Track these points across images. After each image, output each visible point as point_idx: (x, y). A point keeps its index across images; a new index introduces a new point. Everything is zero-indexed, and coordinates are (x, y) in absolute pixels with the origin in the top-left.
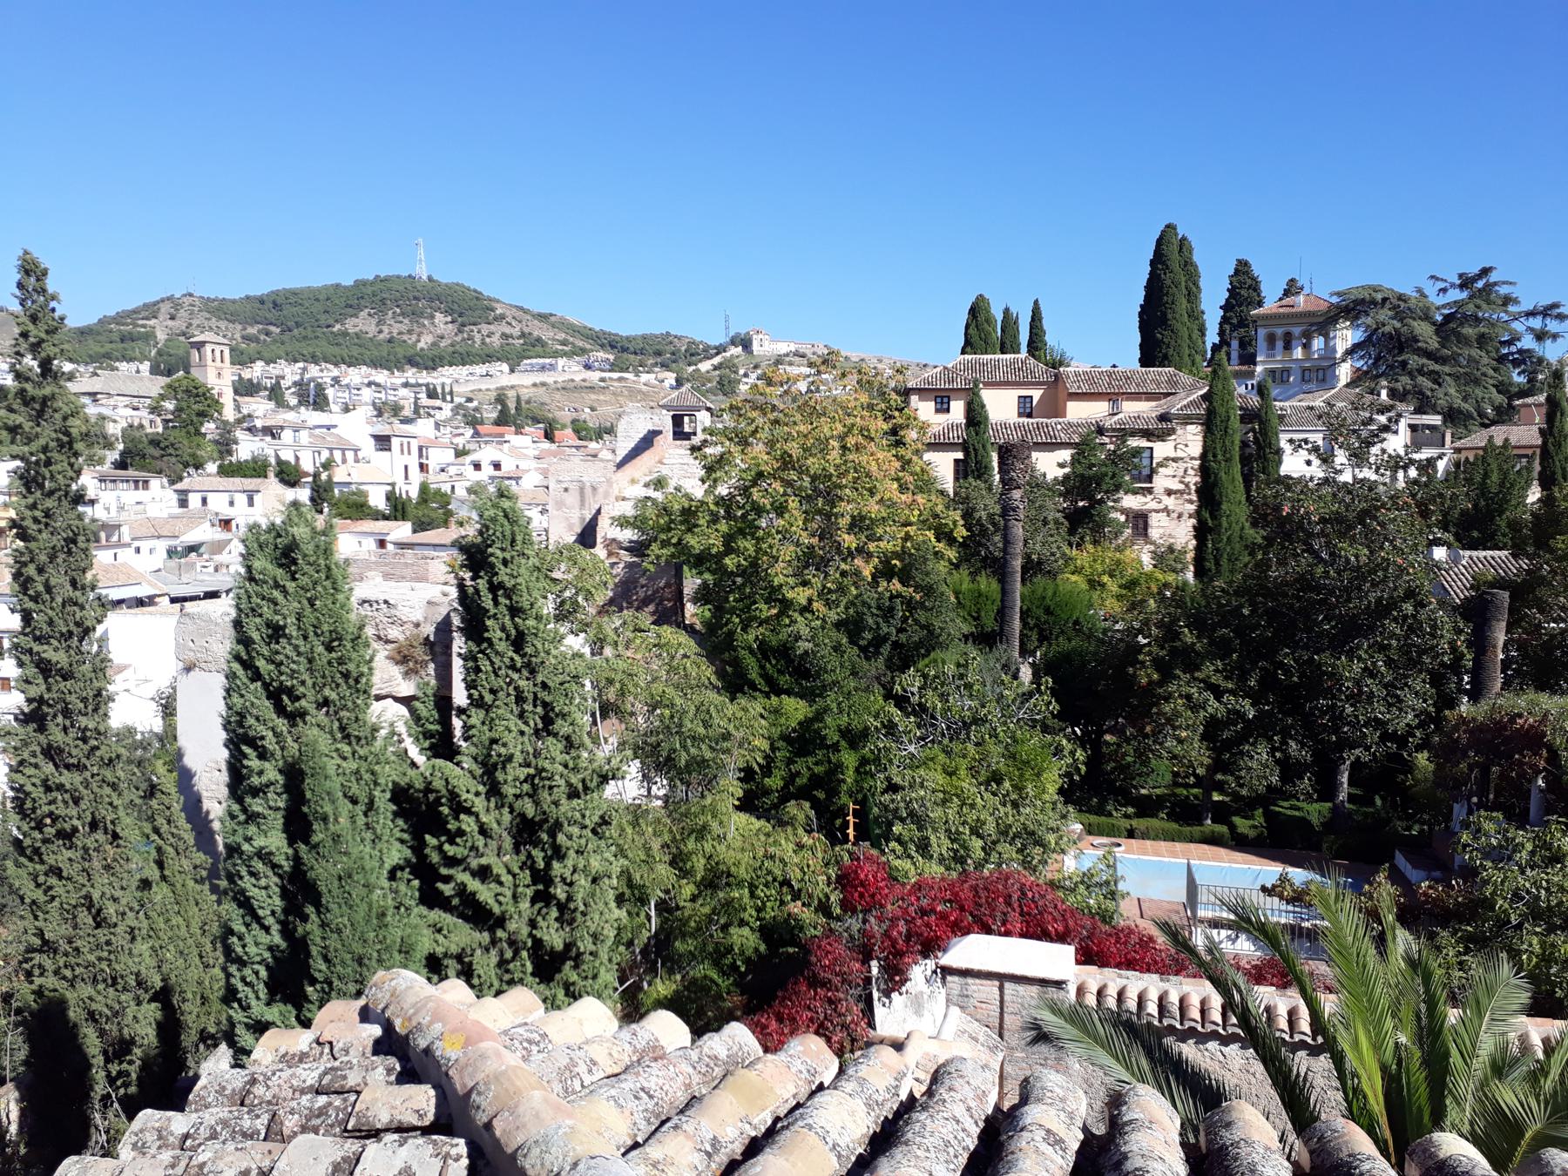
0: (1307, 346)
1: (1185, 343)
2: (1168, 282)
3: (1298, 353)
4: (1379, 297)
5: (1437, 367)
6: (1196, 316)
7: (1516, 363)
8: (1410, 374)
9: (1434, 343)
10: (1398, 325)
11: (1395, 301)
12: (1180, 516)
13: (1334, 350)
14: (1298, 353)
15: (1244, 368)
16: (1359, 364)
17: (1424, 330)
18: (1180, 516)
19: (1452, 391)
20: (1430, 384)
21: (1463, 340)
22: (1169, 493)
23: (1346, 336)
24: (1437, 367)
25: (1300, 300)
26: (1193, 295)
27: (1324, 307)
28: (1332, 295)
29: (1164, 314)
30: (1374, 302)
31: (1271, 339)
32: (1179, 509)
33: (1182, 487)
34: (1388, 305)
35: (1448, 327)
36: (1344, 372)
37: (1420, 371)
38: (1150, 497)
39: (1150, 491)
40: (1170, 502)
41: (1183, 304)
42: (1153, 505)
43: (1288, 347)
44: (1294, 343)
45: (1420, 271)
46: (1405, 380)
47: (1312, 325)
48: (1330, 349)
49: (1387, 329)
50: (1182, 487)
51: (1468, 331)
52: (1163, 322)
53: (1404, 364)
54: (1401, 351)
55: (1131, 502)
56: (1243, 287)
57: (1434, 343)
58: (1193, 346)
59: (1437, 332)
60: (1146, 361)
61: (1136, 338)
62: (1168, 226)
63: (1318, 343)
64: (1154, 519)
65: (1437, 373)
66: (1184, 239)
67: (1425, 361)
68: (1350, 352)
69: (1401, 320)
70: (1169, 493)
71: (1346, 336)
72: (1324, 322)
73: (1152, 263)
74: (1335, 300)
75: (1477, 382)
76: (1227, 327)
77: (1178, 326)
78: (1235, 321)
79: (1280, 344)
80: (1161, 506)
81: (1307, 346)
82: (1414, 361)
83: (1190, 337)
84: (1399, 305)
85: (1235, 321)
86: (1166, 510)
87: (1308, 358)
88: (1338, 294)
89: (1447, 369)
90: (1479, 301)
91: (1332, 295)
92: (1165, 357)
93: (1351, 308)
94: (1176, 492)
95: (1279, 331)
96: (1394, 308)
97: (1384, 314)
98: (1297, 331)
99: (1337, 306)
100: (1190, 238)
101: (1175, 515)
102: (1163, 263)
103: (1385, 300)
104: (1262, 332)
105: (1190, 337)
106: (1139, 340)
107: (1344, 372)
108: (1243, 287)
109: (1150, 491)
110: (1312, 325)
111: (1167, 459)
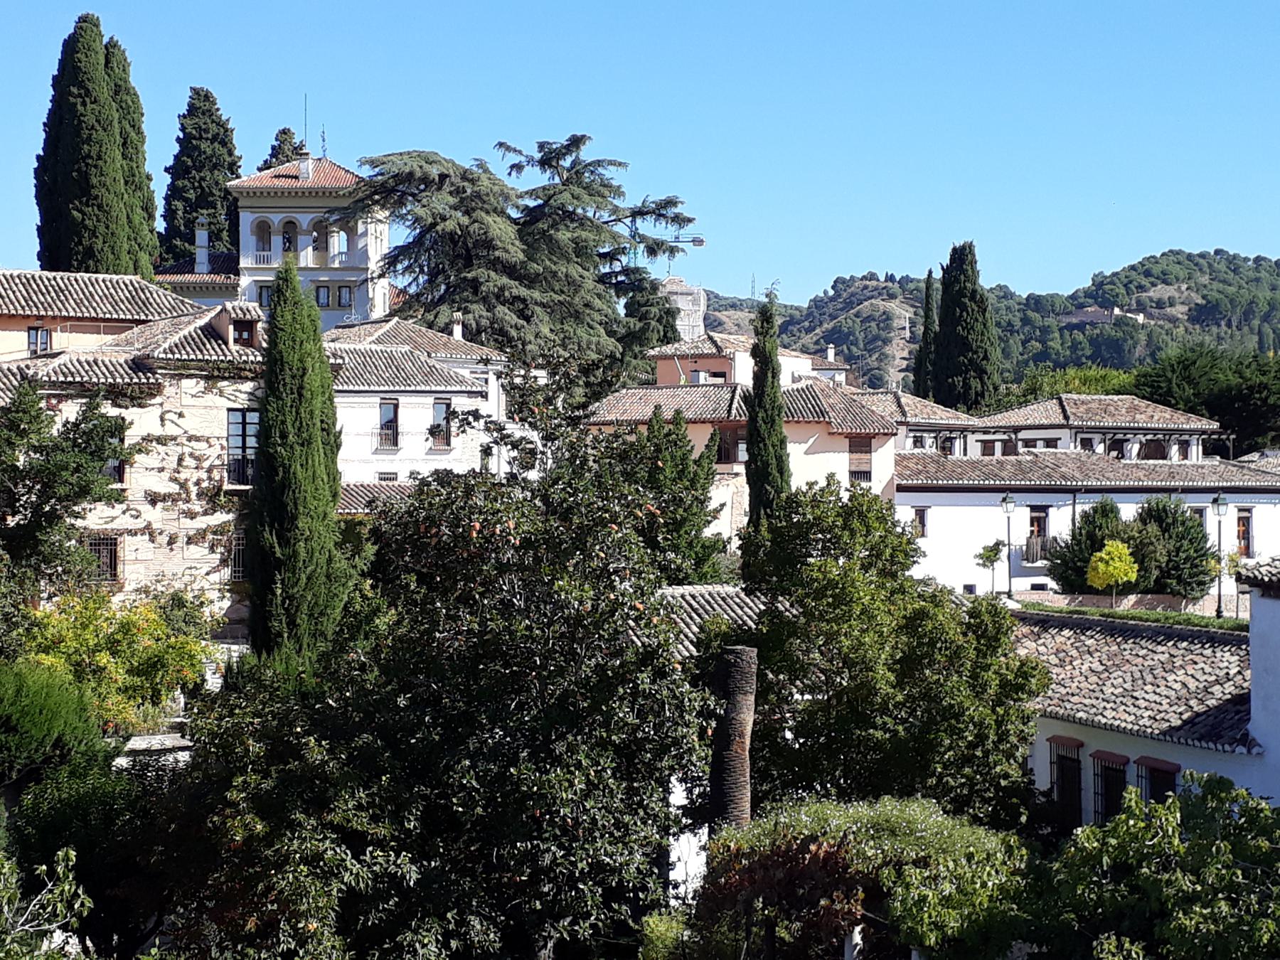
0: (321, 245)
1: (123, 232)
2: (90, 119)
3: (307, 257)
4: (434, 172)
5: (523, 292)
6: (137, 181)
7: (620, 289)
8: (485, 300)
9: (516, 253)
10: (465, 220)
11: (457, 180)
12: (172, 541)
13: (365, 255)
14: (307, 257)
15: (220, 279)
16: (402, 282)
17: (502, 231)
18: (172, 541)
19: (545, 330)
20: (512, 318)
21: (555, 248)
22: (154, 499)
23: (383, 234)
24: (523, 292)
25: (307, 169)
26: (131, 145)
27: (347, 182)
28: (362, 163)
29: (85, 177)
30: (426, 180)
31: (263, 232)
32: (171, 528)
33: (174, 488)
34: (447, 187)
35: (538, 222)
36: (381, 295)
37: (499, 296)
38: (120, 508)
39: (119, 497)
40: (154, 515)
41: (115, 162)
42: (125, 522)
43: (290, 244)
44: (301, 239)
45: (486, 132)
46: (478, 309)
47: (331, 211)
48: (357, 256)
49: (450, 225)
50: (174, 488)
51: (564, 236)
52: (84, 190)
53: (475, 285)
54: (469, 265)
55: (96, 517)
56: (204, 134)
57: (516, 253)
58: (135, 236)
59: (521, 235)
60: (52, 257)
61: (32, 216)
62: (83, 19)
63: (338, 242)
64: (129, 548)
65: (524, 301)
66: (112, 46)
67: (505, 280)
68: (392, 260)
69: (467, 213)
70: (154, 499)
71: (383, 234)
72: (349, 206)
73: (56, 82)
74: (366, 172)
75: (577, 317)
76: (179, 205)
77: (108, 198)
78: (191, 195)
79: (277, 241)
80: (140, 524)
81: (321, 245)
82: (495, 281)
83: (130, 221)
84: (470, 192)
85: (191, 195)
86: (149, 531)
87: (324, 268)
88: (373, 163)
89: (536, 295)
90: (577, 190)
91: (362, 163)
92: (90, 253)
93: (393, 188)
94: (164, 498)
95: (276, 219)
96: (458, 191)
97: (441, 201)
98: (304, 220)
99: (369, 183)
100: (123, 44)
101: (163, 539)
102: (81, 85)
103: (443, 177)
104: (246, 220)
105: (130, 221)
106: (36, 219)
107: (381, 295)
108: (204, 134)
109: (119, 497)
110: (331, 211)
111: (148, 439)
